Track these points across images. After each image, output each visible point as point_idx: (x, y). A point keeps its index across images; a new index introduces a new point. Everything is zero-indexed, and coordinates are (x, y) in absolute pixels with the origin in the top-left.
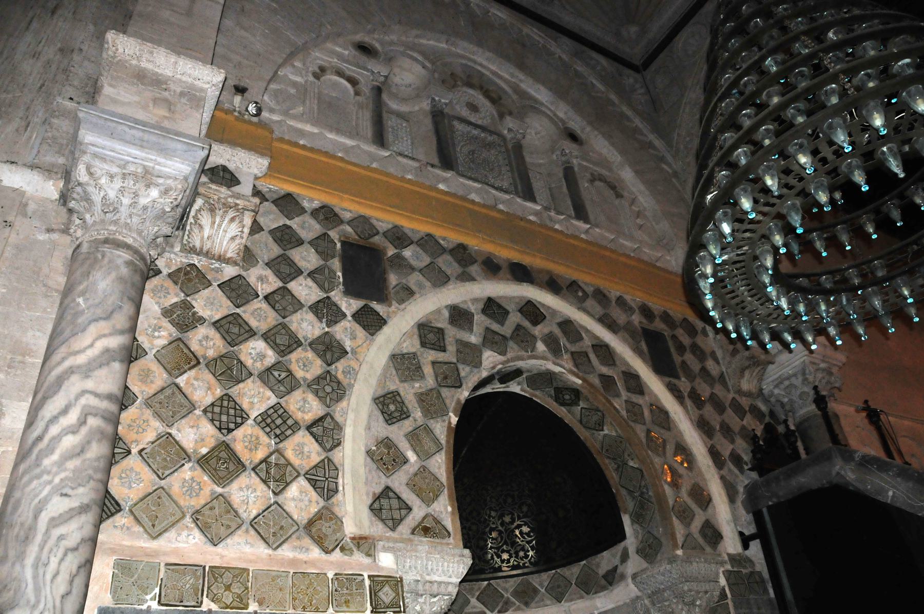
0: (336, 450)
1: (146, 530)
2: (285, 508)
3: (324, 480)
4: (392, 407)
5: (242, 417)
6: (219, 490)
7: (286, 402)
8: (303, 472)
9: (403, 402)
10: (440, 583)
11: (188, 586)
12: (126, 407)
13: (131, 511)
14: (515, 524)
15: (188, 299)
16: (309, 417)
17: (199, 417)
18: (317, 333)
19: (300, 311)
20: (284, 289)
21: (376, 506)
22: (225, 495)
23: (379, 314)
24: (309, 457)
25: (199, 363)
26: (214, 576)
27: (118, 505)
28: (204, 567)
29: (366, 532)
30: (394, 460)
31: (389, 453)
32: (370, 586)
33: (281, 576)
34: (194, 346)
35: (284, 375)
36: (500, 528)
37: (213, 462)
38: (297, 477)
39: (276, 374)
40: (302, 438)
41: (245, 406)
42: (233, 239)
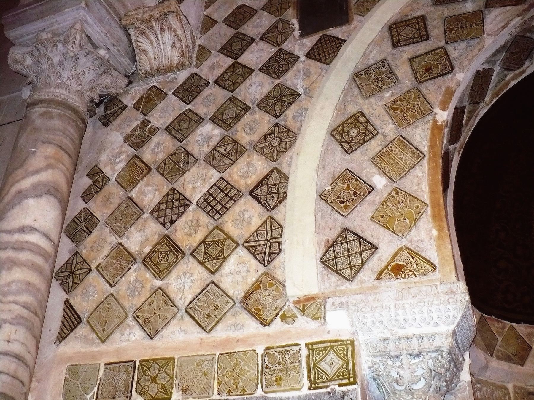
0: (281, 207)
1: (98, 336)
2: (221, 285)
3: (266, 246)
6: (158, 283)
7: (230, 174)
8: (241, 242)
9: (368, 122)
10: (420, 337)
11: (121, 382)
12: (91, 232)
13: (88, 321)
15: (147, 117)
17: (147, 218)
19: (250, 77)
21: (330, 255)
22: (163, 287)
23: (338, 38)
24: (249, 223)
25: (150, 169)
26: (142, 368)
27: (80, 318)
28: (136, 361)
29: (313, 289)
30: (355, 194)
31: (348, 188)
32: (308, 357)
33: (206, 360)
35: (229, 147)
37: (155, 258)
38: (236, 248)
39: (222, 150)
42: (173, 45)
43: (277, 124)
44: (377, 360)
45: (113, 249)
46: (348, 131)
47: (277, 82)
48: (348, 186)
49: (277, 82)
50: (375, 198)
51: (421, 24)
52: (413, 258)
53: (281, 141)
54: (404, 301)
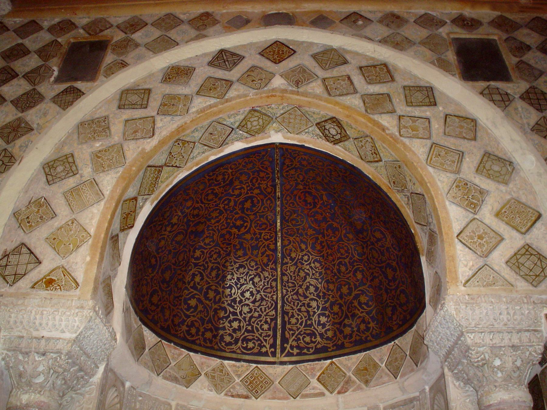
9: (74, 162)
10: (48, 339)
14: (353, 294)
36: (340, 301)
43: (5, 150)
44: (10, 354)
46: (57, 167)
47: (20, 115)
48: (39, 210)
49: (20, 115)
50: (56, 223)
51: (146, 95)
52: (64, 276)
53: (3, 163)
54: (44, 309)
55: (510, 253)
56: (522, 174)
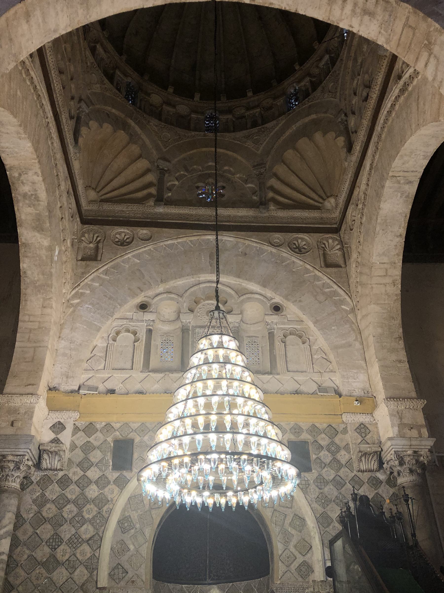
0: (98, 551)
4: (126, 525)
5: (61, 542)
9: (132, 521)
12: (17, 547)
16: (88, 536)
18: (96, 494)
20: (84, 475)
21: (112, 573)
34: (44, 514)
35: (80, 518)
40: (86, 547)
41: (62, 537)
45: (28, 557)
55: (297, 565)
56: (307, 526)
